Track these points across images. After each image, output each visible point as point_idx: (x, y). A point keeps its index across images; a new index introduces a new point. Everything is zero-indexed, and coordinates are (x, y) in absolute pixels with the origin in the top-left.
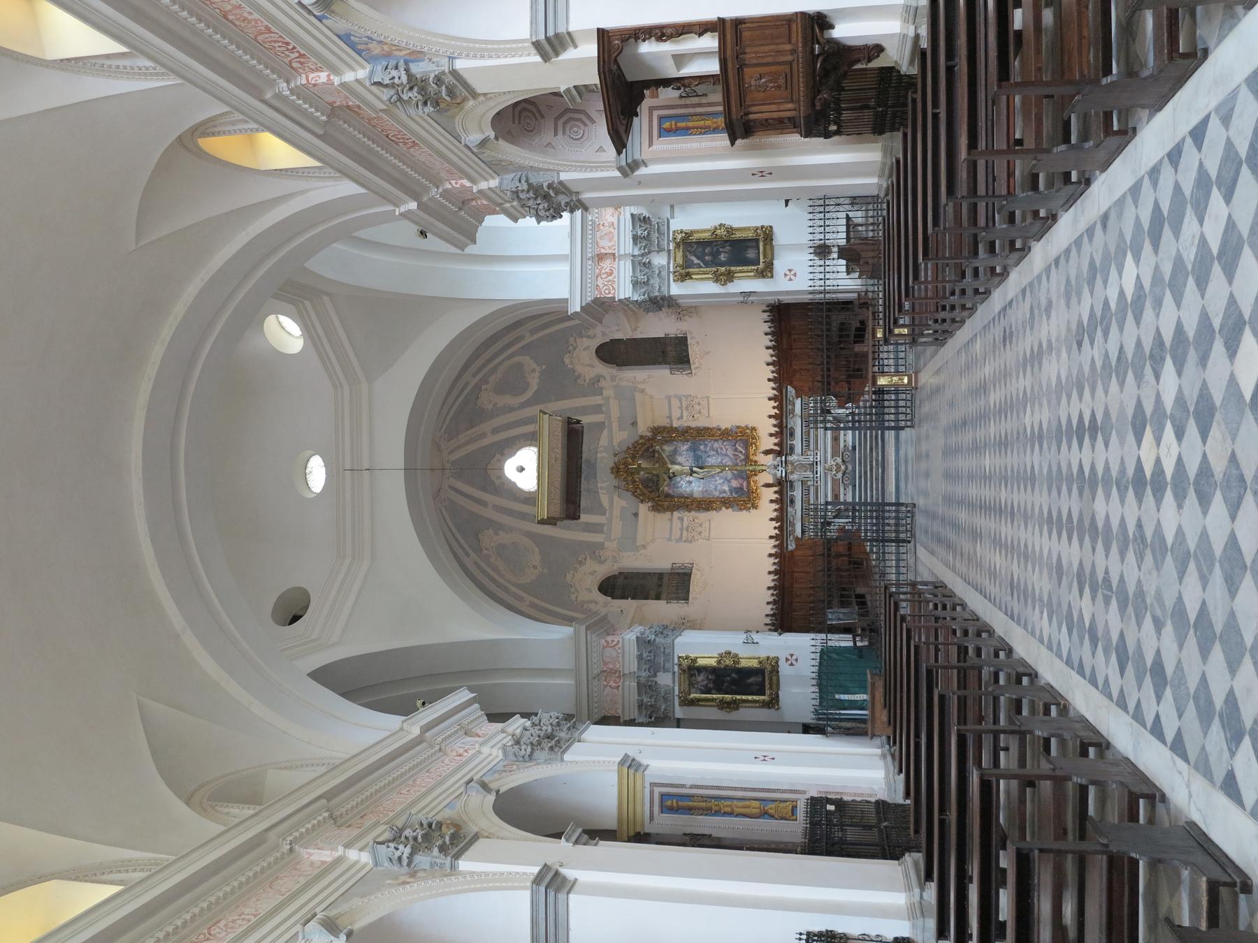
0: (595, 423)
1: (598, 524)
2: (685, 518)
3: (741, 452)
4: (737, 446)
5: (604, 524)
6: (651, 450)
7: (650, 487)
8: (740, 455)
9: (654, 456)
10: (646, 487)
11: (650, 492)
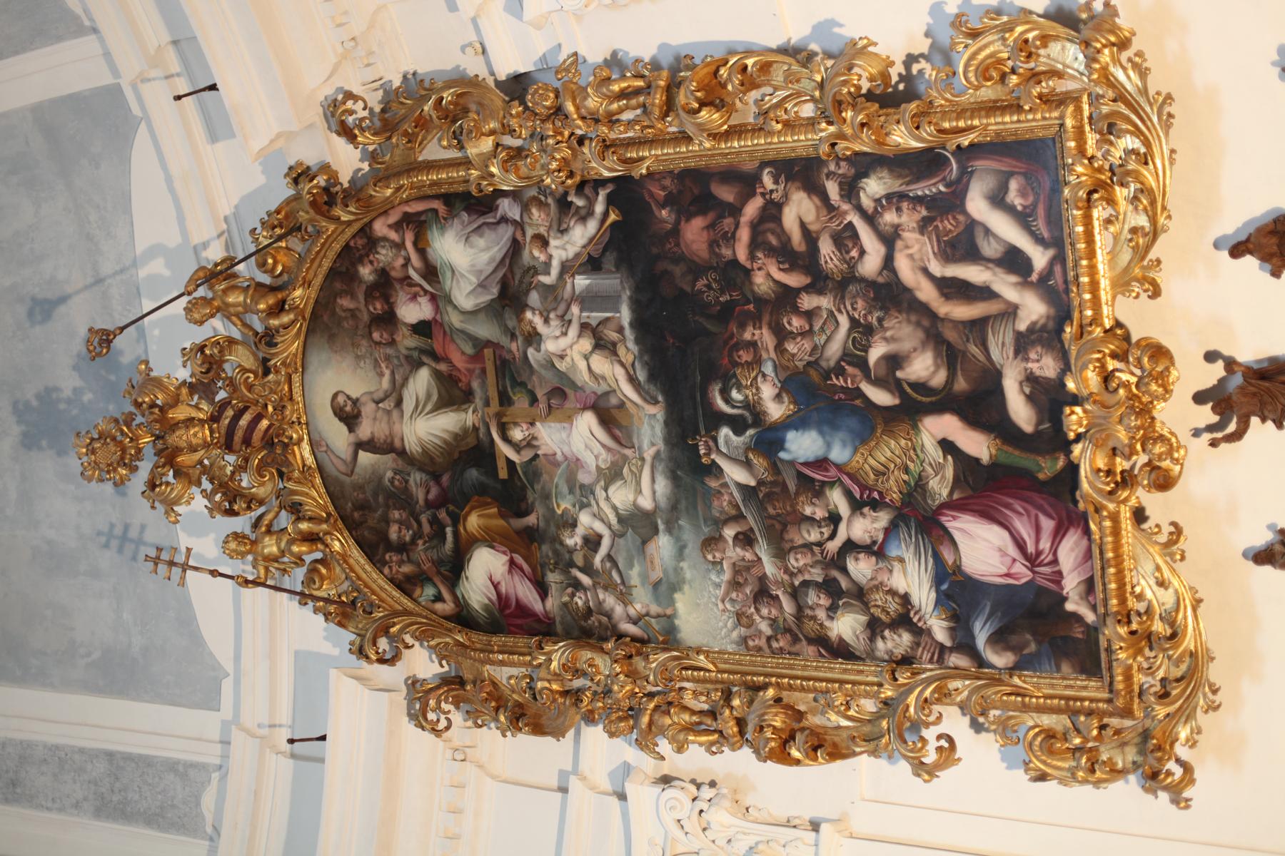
0: (77, 103)
1: (173, 766)
2: (642, 794)
3: (1014, 261)
4: (977, 205)
5: (202, 767)
6: (366, 272)
7: (402, 548)
8: (1006, 286)
9: (388, 319)
10: (375, 548)
11: (405, 585)
